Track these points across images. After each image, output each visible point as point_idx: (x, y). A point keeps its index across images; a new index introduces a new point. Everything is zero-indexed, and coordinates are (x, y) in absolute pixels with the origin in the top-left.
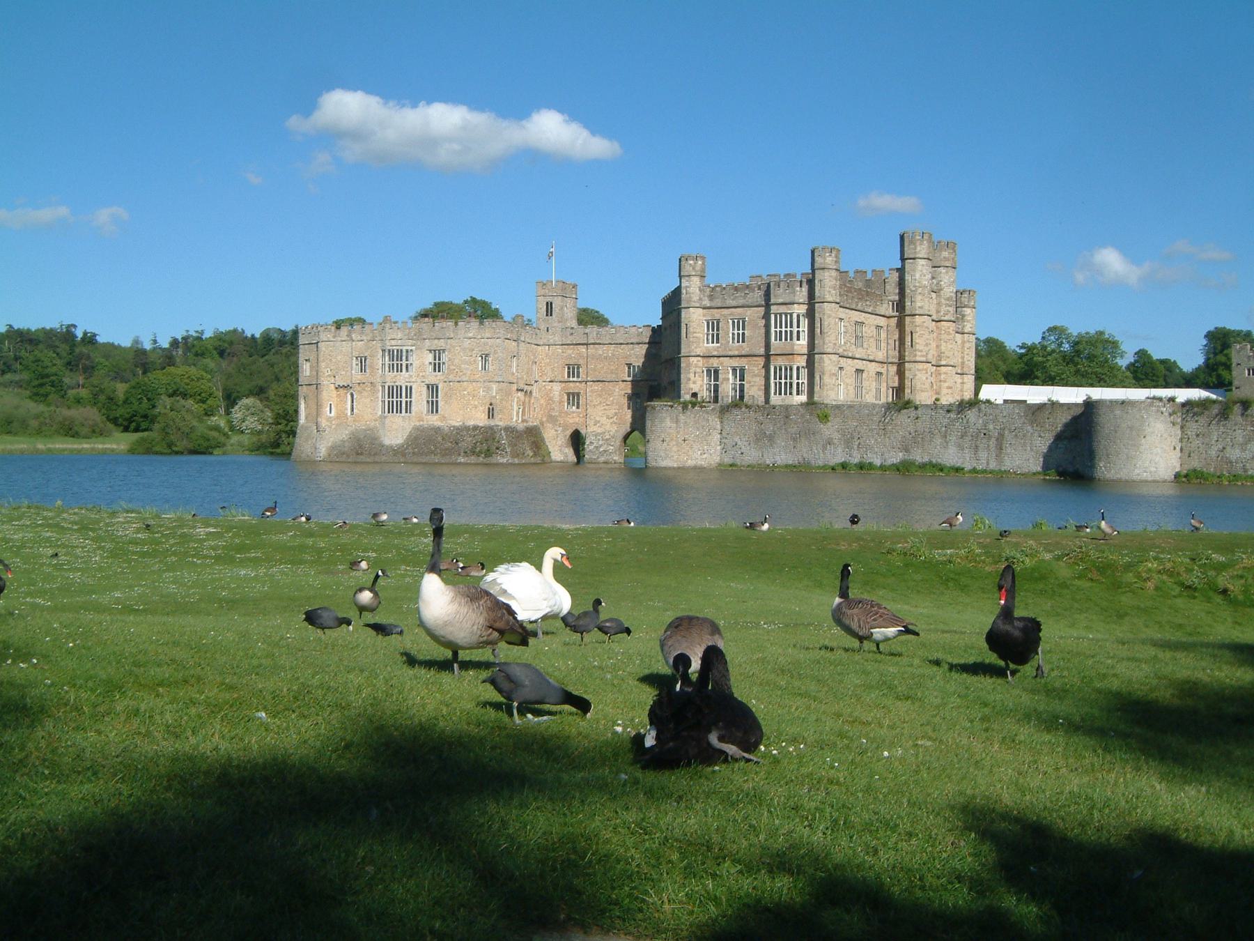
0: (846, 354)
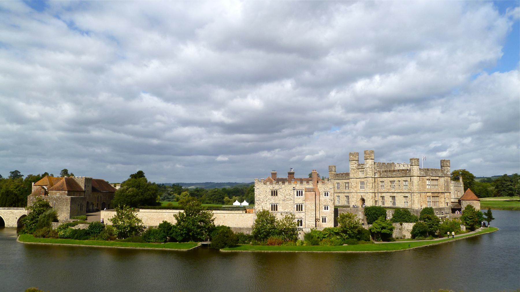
0: (341, 192)
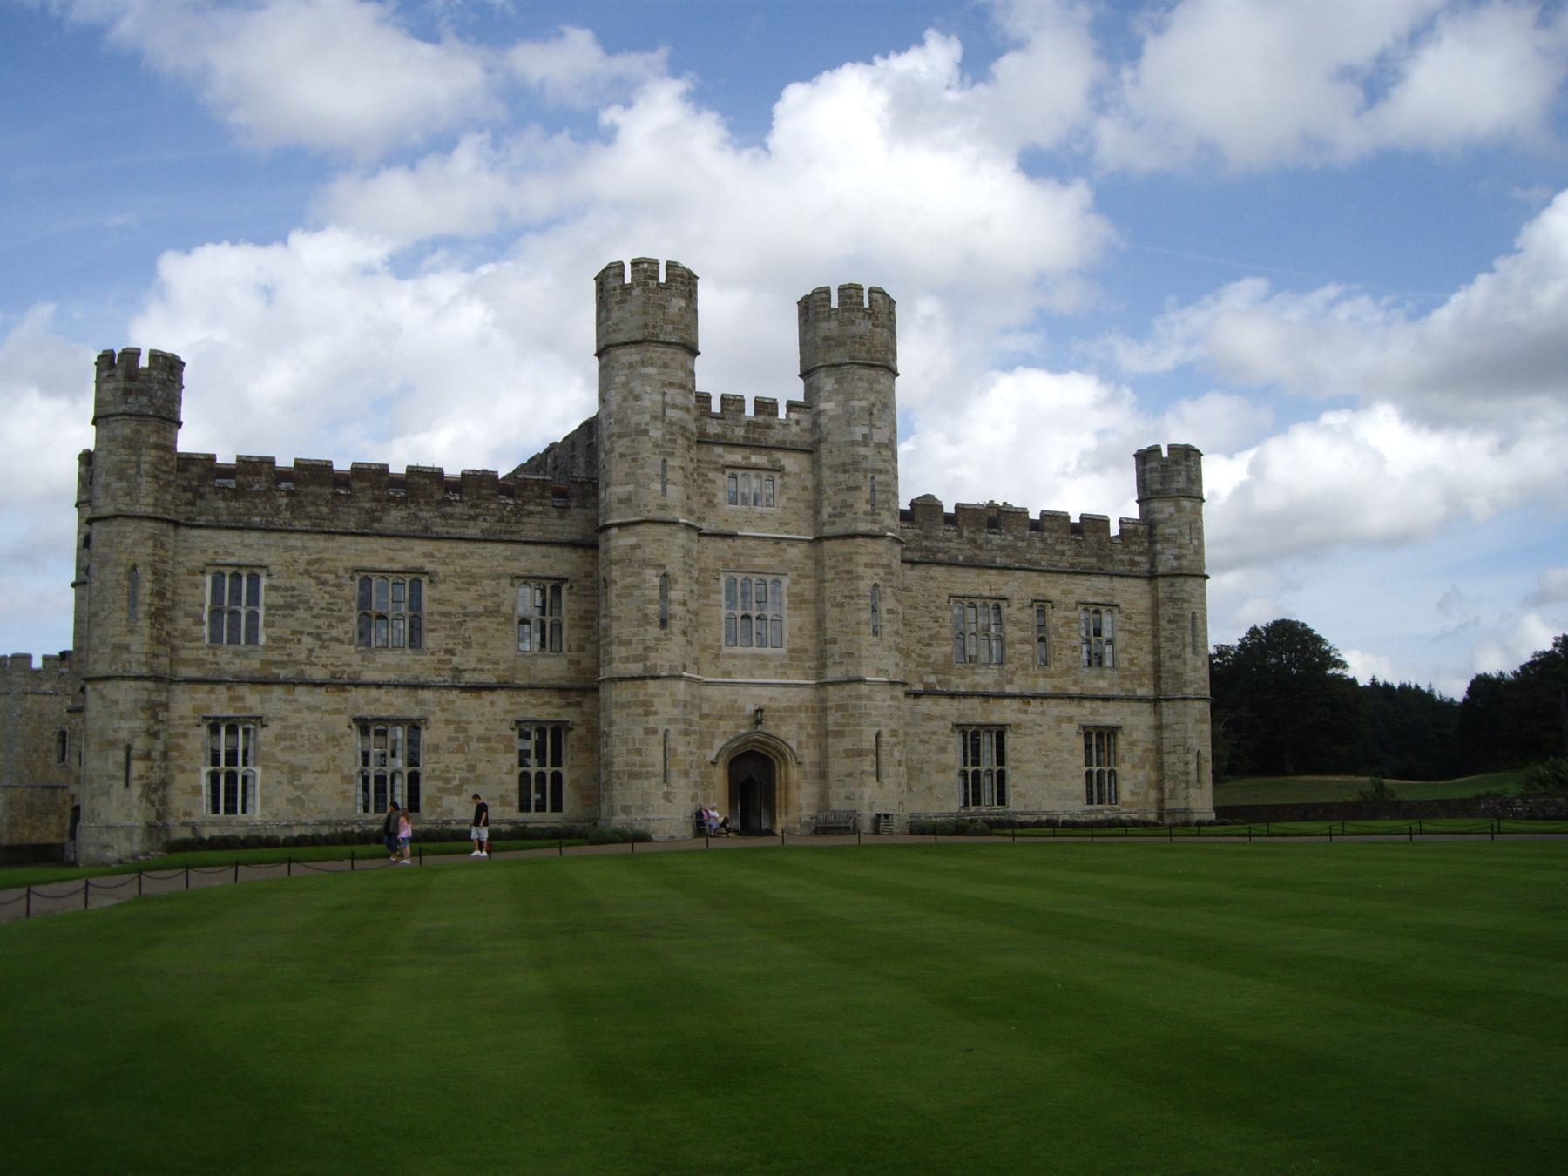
0: (283, 673)
